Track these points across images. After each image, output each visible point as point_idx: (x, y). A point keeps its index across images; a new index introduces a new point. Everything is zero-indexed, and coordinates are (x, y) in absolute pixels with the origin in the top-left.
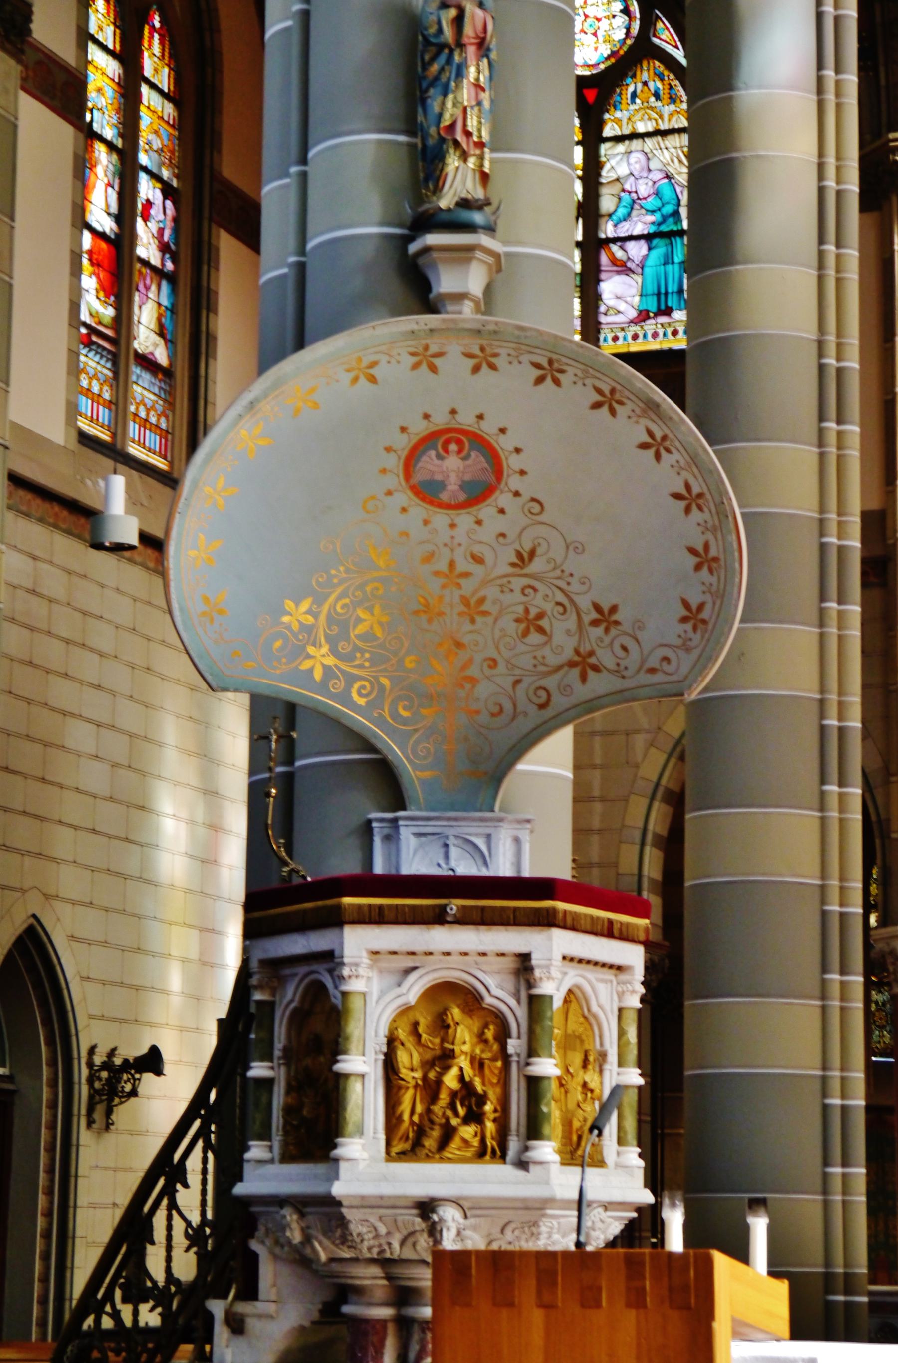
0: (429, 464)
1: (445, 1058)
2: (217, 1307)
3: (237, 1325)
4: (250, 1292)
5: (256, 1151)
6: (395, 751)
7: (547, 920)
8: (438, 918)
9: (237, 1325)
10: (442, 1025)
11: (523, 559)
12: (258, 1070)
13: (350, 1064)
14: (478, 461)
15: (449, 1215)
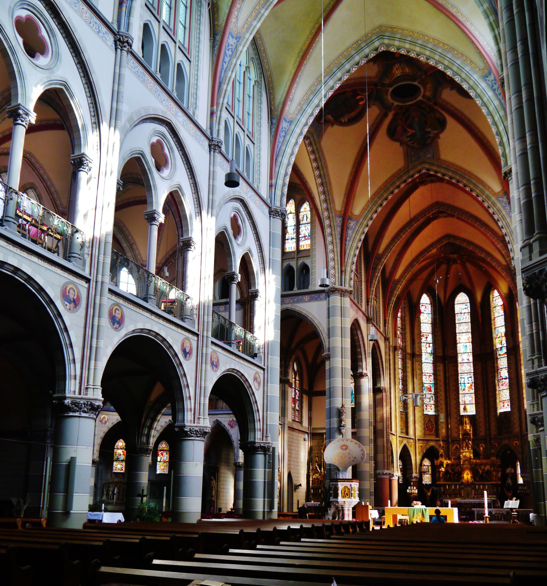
0: (343, 447)
1: (345, 491)
2: (328, 509)
3: (330, 510)
4: (331, 507)
5: (331, 498)
6: (339, 467)
7: (352, 482)
8: (345, 482)
9: (330, 510)
10: (345, 489)
11: (349, 453)
12: (331, 492)
13: (339, 492)
14: (346, 447)
15: (346, 502)
